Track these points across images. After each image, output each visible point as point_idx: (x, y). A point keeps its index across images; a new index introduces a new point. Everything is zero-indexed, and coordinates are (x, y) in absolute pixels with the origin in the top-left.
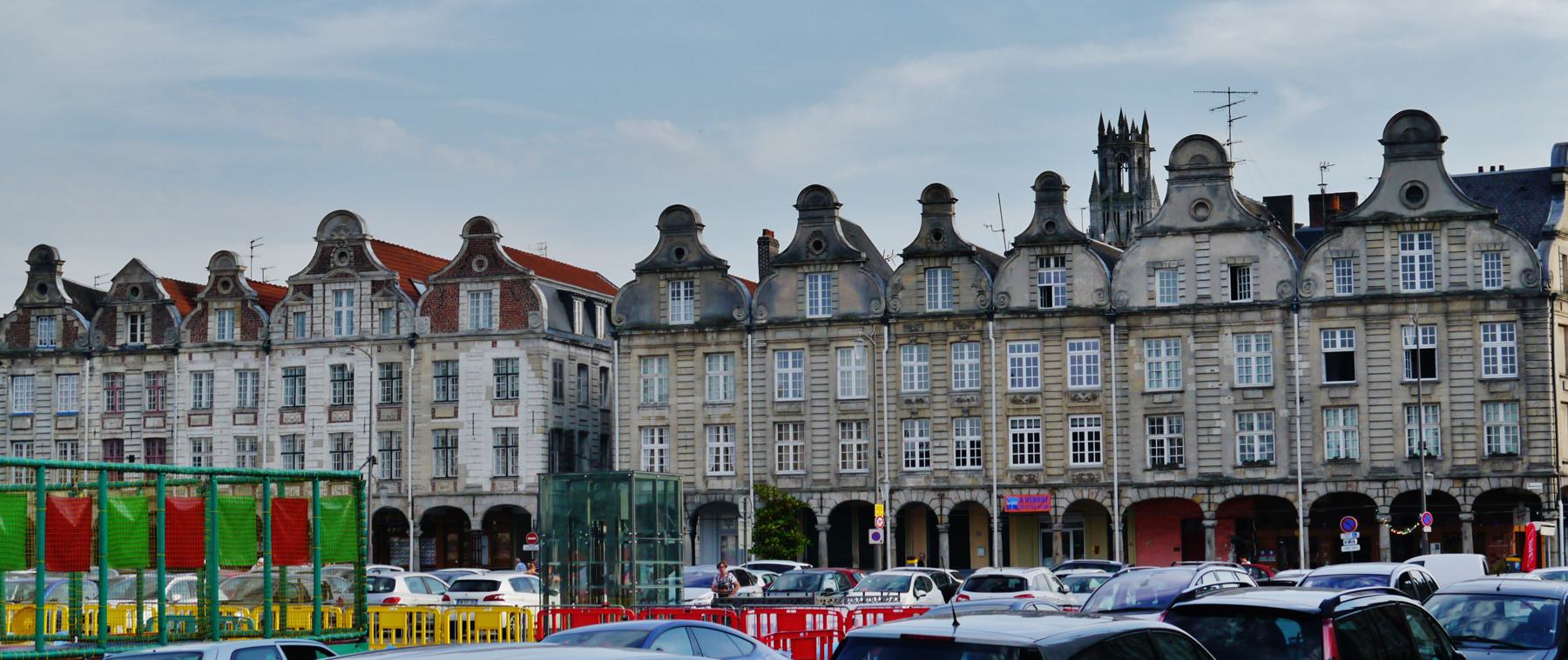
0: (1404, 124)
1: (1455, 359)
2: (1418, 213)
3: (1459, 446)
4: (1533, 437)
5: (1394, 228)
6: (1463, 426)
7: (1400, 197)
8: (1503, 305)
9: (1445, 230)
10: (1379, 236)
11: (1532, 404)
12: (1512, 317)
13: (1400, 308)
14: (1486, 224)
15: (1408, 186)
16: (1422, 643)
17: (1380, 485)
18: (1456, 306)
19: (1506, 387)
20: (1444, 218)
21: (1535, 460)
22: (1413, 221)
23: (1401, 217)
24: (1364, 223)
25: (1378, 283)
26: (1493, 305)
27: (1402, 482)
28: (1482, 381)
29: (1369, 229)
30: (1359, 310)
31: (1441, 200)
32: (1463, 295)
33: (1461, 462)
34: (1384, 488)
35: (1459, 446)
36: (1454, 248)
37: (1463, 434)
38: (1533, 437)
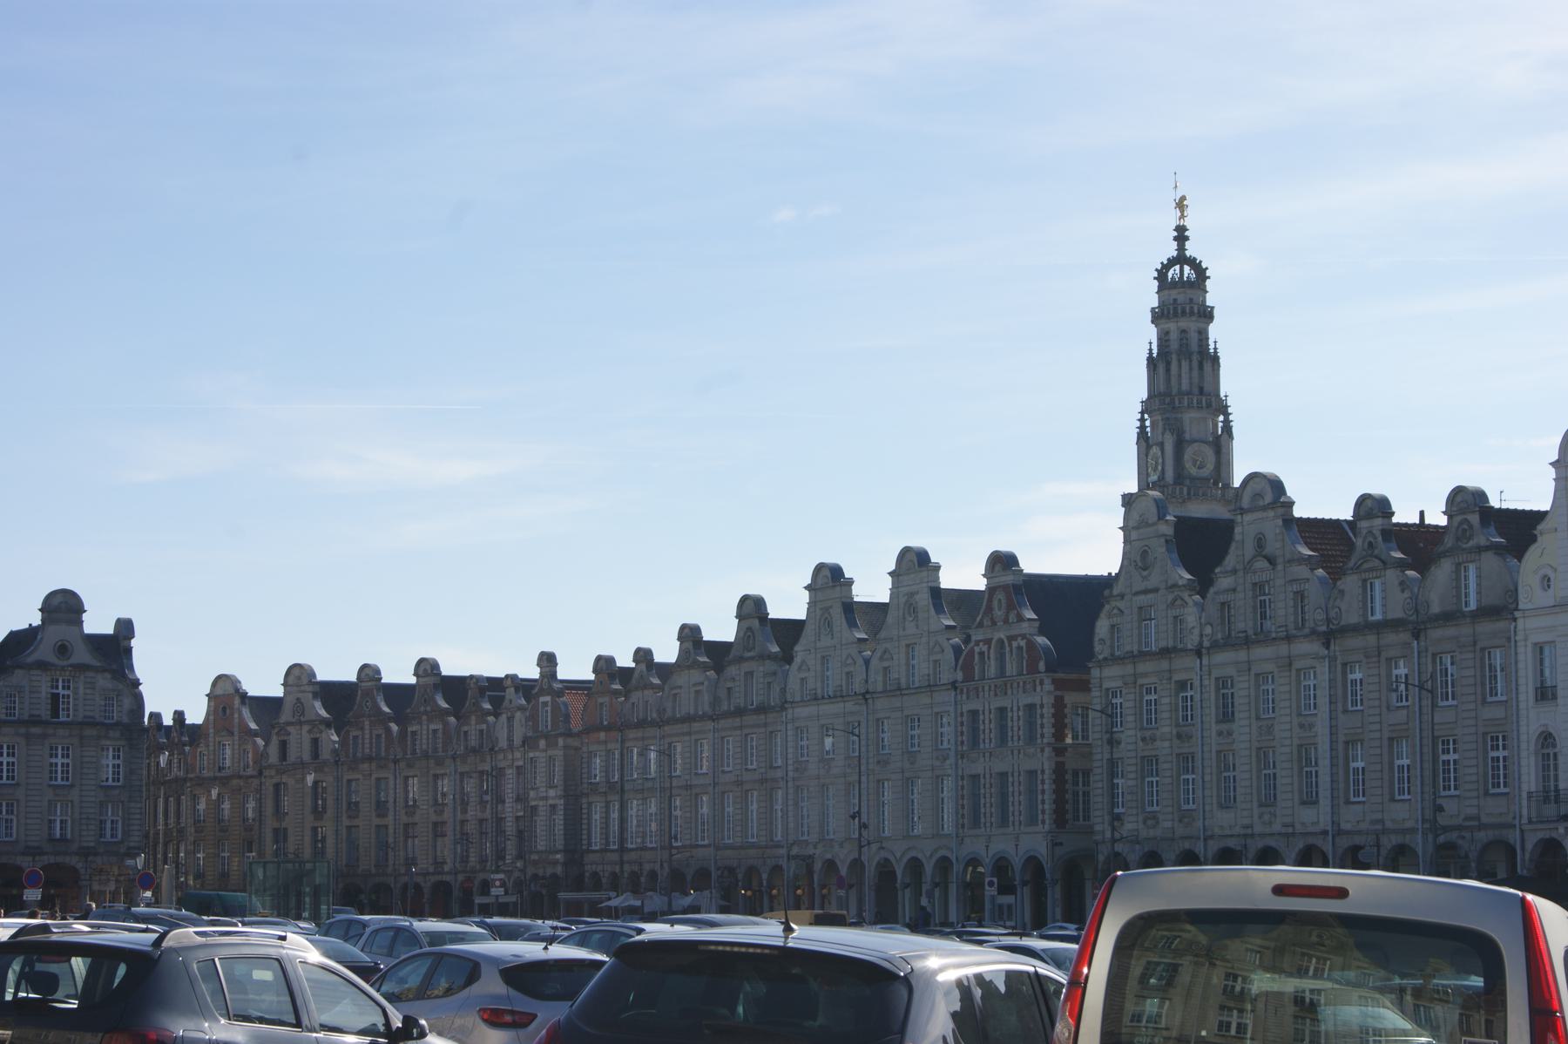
0: (59, 599)
1: (85, 771)
2: (65, 663)
3: (84, 833)
4: (132, 828)
5: (49, 673)
6: (88, 819)
7: (54, 649)
8: (118, 734)
9: (82, 677)
10: (39, 678)
11: (132, 805)
12: (123, 743)
13: (50, 731)
14: (108, 676)
15: (60, 643)
16: (14, 971)
17: (31, 859)
18: (88, 732)
19: (117, 792)
20: (82, 668)
21: (132, 844)
22: (63, 669)
23: (53, 665)
24: (30, 667)
25: (37, 713)
26: (111, 734)
27: (46, 857)
28: (102, 787)
29: (32, 672)
30: (23, 730)
31: (82, 655)
32: (93, 724)
33: (85, 844)
34: (34, 861)
35: (84, 833)
36: (88, 691)
37: (87, 825)
38: (132, 828)
